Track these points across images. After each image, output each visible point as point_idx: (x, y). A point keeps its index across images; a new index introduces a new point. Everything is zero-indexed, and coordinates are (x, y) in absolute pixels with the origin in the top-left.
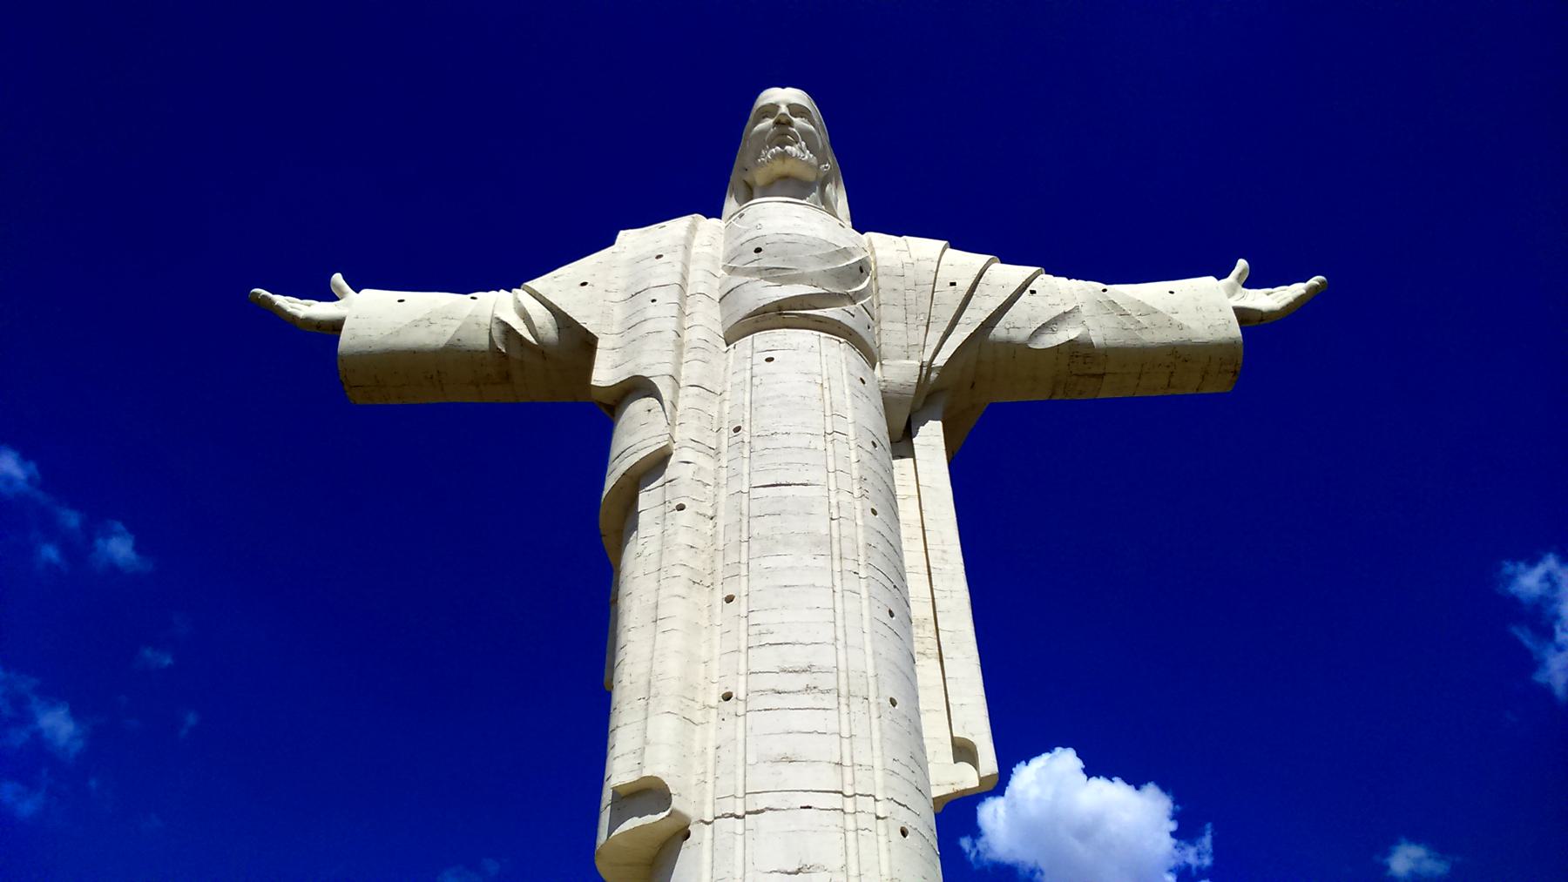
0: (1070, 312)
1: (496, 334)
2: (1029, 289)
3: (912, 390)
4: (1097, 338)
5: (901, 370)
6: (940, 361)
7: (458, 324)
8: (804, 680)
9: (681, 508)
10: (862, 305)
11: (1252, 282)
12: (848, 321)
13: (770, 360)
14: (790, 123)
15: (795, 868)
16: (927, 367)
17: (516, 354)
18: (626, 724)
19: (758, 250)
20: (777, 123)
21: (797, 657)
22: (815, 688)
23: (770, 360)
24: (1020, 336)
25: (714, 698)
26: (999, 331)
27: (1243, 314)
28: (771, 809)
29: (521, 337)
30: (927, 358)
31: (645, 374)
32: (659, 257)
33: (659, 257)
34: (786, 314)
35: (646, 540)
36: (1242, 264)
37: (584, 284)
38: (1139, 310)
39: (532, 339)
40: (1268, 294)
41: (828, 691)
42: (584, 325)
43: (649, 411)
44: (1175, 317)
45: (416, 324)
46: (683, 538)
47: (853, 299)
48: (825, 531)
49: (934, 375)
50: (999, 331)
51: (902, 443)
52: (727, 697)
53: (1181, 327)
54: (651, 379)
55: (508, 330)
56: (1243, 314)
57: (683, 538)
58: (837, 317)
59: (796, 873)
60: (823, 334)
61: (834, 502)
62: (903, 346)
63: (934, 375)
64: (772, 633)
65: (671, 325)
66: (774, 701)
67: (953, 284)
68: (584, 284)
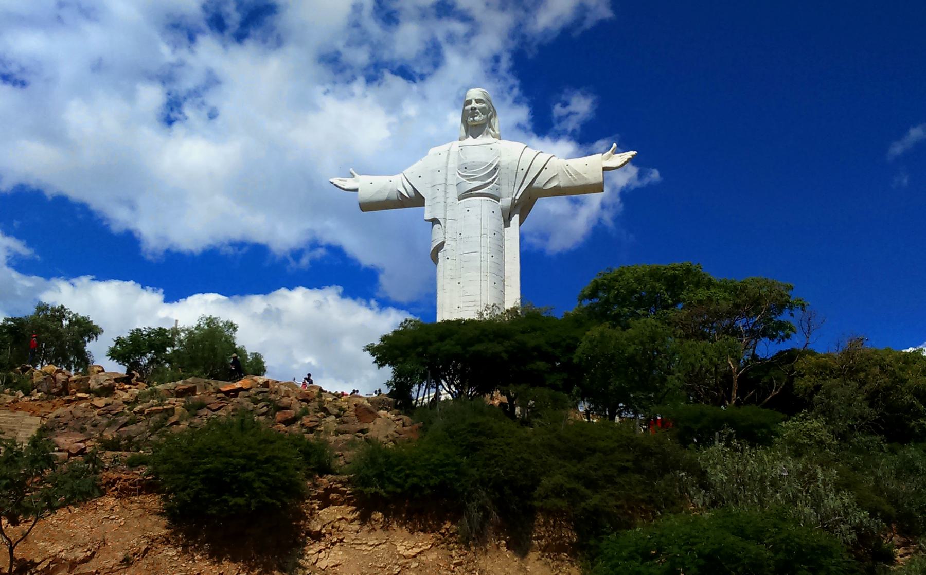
1: (398, 195)
2: (545, 167)
3: (509, 207)
4: (562, 185)
5: (506, 202)
6: (517, 197)
7: (388, 191)
8: (474, 303)
9: (448, 258)
10: (496, 183)
11: (615, 152)
12: (490, 192)
13: (468, 211)
14: (475, 109)
20: (472, 109)
21: (472, 298)
23: (468, 211)
24: (541, 185)
25: (457, 307)
29: (406, 197)
30: (514, 197)
31: (438, 218)
37: (420, 177)
40: (621, 156)
44: (584, 175)
45: (377, 193)
46: (449, 267)
47: (491, 182)
48: (479, 265)
49: (516, 201)
50: (535, 185)
51: (507, 223)
52: (459, 307)
53: (586, 179)
55: (401, 194)
57: (449, 267)
61: (482, 256)
63: (516, 201)
65: (443, 199)
66: (467, 308)
67: (522, 169)
68: (420, 177)
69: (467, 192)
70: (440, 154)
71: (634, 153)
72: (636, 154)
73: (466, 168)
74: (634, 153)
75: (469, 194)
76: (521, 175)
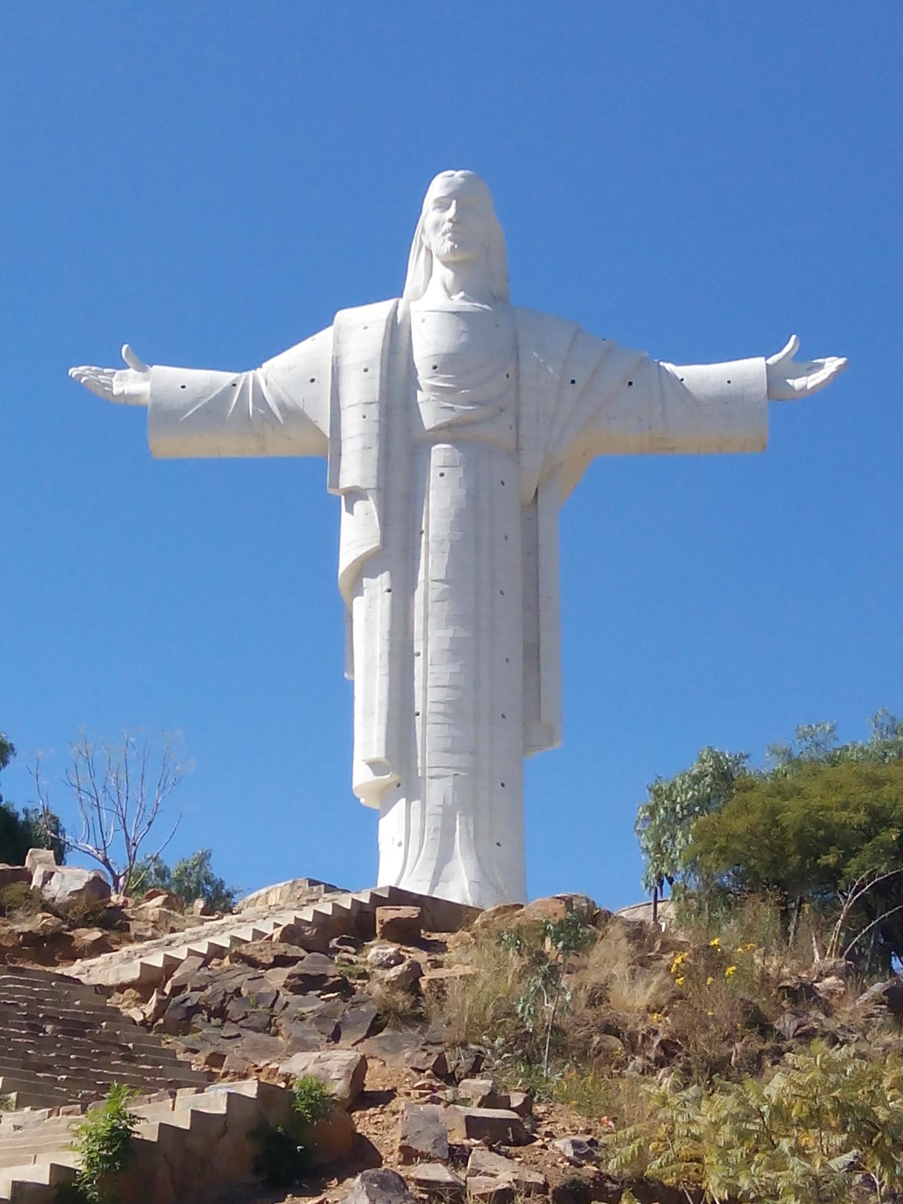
9: (389, 591)
13: (442, 475)
20: (450, 220)
23: (442, 475)
33: (366, 370)
37: (313, 380)
66: (440, 719)
68: (313, 380)
70: (366, 328)
71: (842, 361)
72: (846, 364)
74: (842, 361)
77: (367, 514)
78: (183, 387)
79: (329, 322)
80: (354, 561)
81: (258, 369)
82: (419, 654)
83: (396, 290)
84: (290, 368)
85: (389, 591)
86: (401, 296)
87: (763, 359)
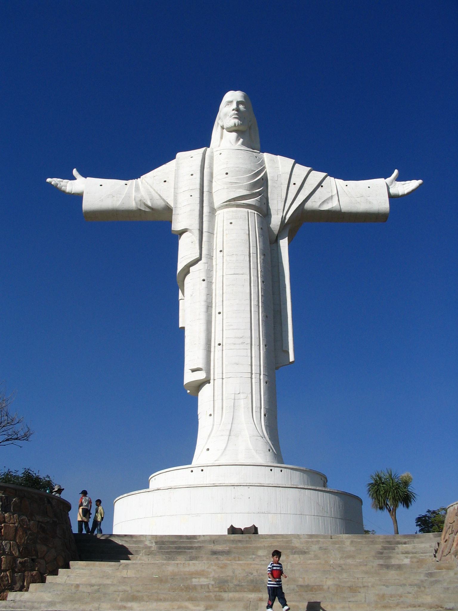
0: (333, 195)
8: (241, 340)
9: (204, 280)
11: (399, 179)
13: (231, 223)
15: (238, 393)
16: (283, 219)
17: (143, 208)
18: (191, 351)
19: (227, 174)
22: (244, 343)
23: (231, 223)
25: (217, 344)
26: (309, 205)
27: (392, 198)
28: (232, 377)
32: (192, 175)
33: (192, 175)
34: (236, 203)
35: (193, 290)
36: (396, 172)
37: (165, 181)
38: (357, 195)
39: (149, 204)
41: (247, 344)
42: (166, 200)
43: (192, 242)
44: (369, 198)
53: (370, 203)
54: (192, 230)
56: (392, 198)
58: (254, 204)
59: (239, 394)
60: (250, 211)
62: (276, 210)
64: (232, 325)
67: (294, 184)
68: (165, 181)
69: (229, 201)
71: (420, 181)
73: (227, 174)
74: (420, 181)
75: (233, 202)
76: (293, 190)
77: (192, 242)
78: (101, 185)
79: (174, 158)
80: (185, 266)
81: (139, 179)
82: (220, 313)
83: (206, 143)
84: (154, 177)
85: (204, 280)
86: (209, 147)
87: (382, 180)
